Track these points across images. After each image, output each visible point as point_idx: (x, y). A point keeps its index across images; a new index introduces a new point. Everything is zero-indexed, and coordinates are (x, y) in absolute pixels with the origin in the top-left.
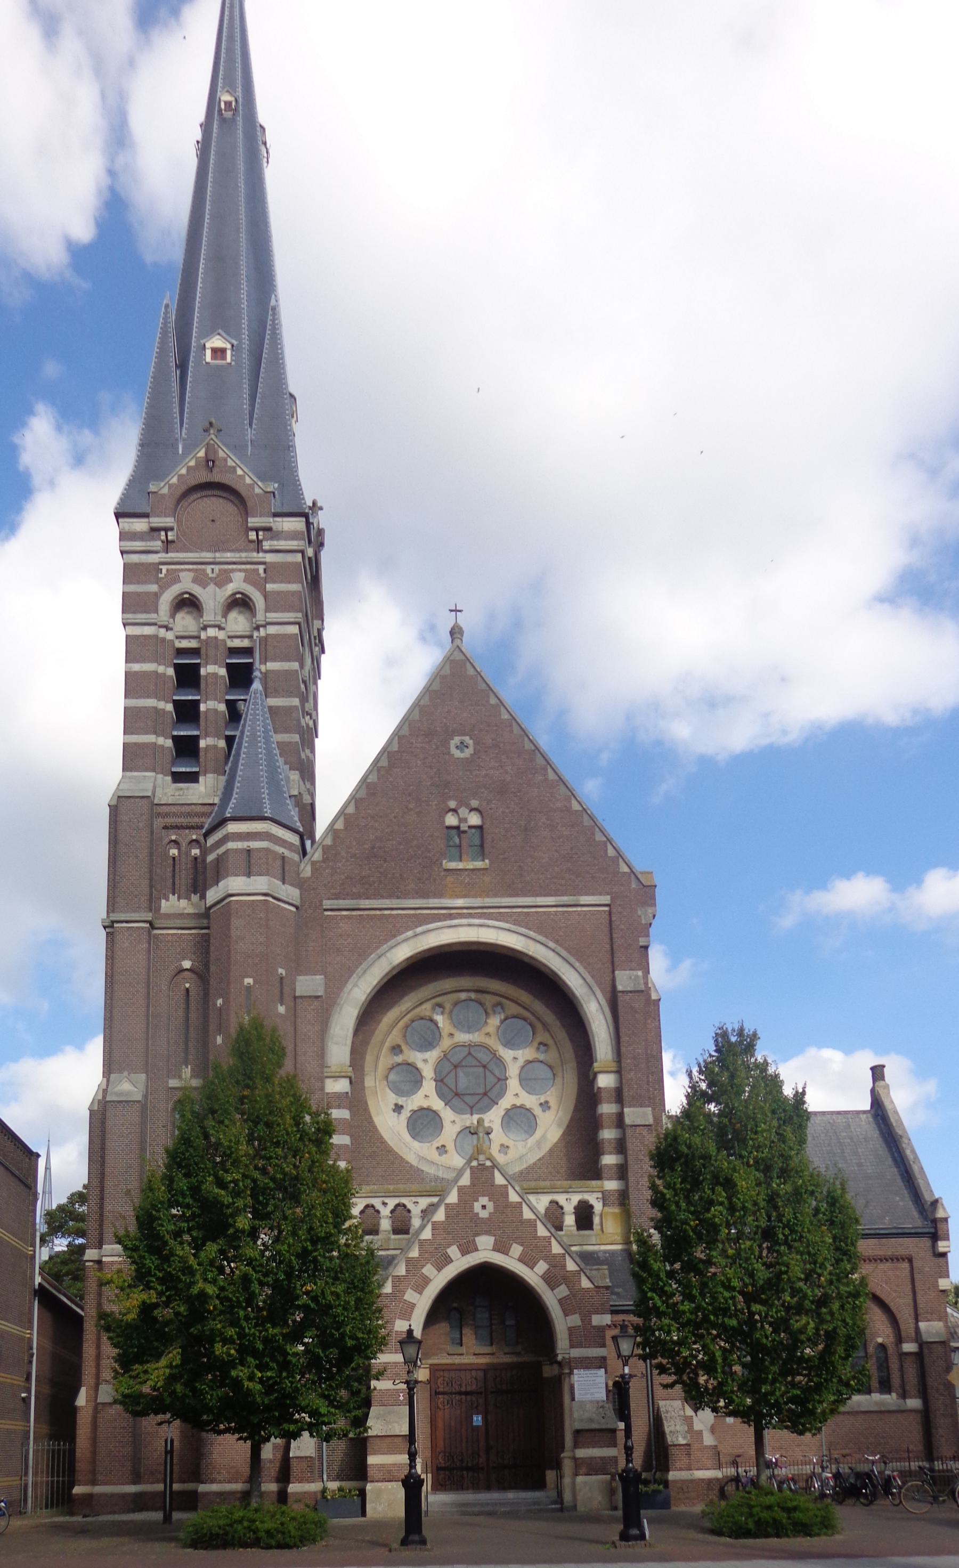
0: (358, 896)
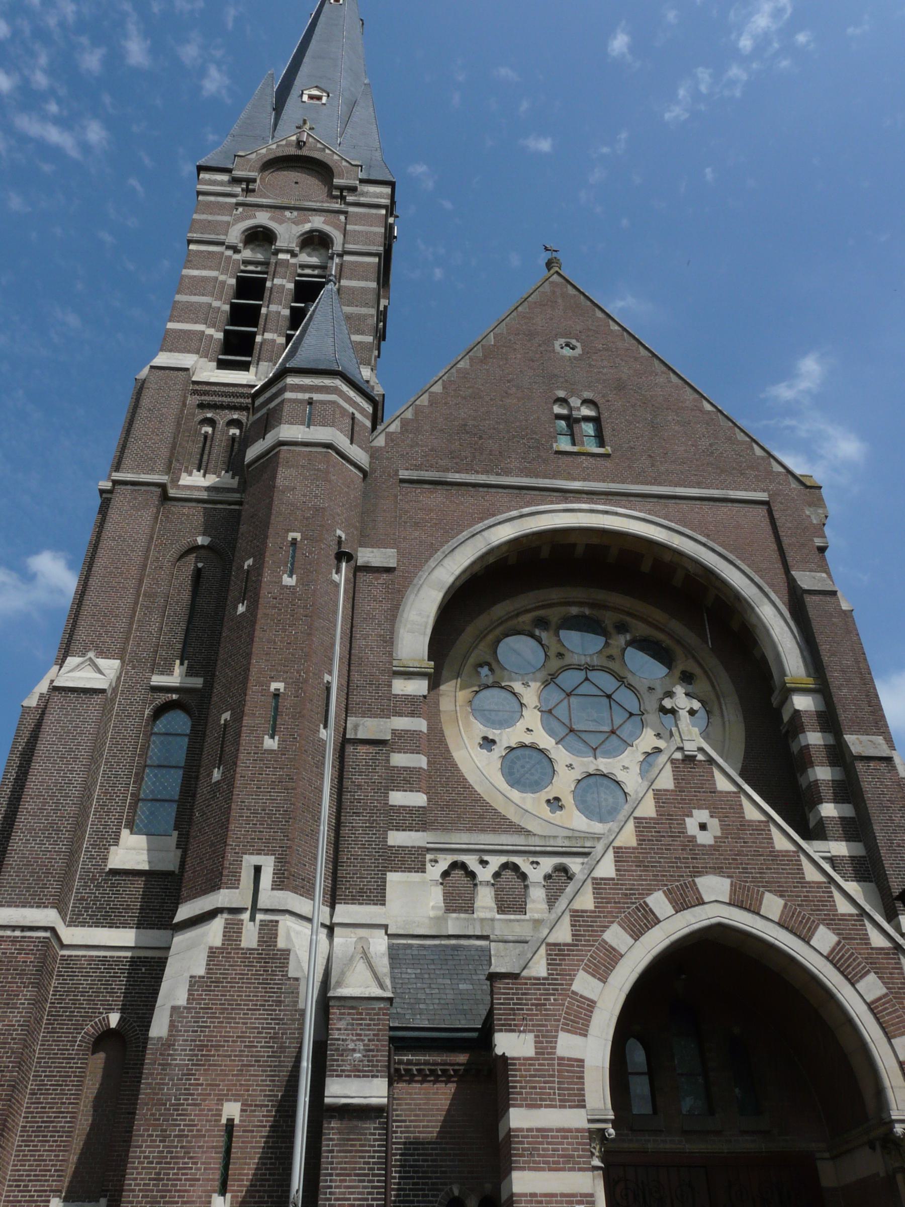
0: (447, 470)
